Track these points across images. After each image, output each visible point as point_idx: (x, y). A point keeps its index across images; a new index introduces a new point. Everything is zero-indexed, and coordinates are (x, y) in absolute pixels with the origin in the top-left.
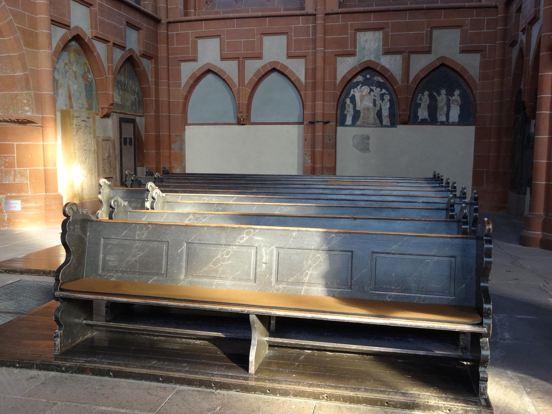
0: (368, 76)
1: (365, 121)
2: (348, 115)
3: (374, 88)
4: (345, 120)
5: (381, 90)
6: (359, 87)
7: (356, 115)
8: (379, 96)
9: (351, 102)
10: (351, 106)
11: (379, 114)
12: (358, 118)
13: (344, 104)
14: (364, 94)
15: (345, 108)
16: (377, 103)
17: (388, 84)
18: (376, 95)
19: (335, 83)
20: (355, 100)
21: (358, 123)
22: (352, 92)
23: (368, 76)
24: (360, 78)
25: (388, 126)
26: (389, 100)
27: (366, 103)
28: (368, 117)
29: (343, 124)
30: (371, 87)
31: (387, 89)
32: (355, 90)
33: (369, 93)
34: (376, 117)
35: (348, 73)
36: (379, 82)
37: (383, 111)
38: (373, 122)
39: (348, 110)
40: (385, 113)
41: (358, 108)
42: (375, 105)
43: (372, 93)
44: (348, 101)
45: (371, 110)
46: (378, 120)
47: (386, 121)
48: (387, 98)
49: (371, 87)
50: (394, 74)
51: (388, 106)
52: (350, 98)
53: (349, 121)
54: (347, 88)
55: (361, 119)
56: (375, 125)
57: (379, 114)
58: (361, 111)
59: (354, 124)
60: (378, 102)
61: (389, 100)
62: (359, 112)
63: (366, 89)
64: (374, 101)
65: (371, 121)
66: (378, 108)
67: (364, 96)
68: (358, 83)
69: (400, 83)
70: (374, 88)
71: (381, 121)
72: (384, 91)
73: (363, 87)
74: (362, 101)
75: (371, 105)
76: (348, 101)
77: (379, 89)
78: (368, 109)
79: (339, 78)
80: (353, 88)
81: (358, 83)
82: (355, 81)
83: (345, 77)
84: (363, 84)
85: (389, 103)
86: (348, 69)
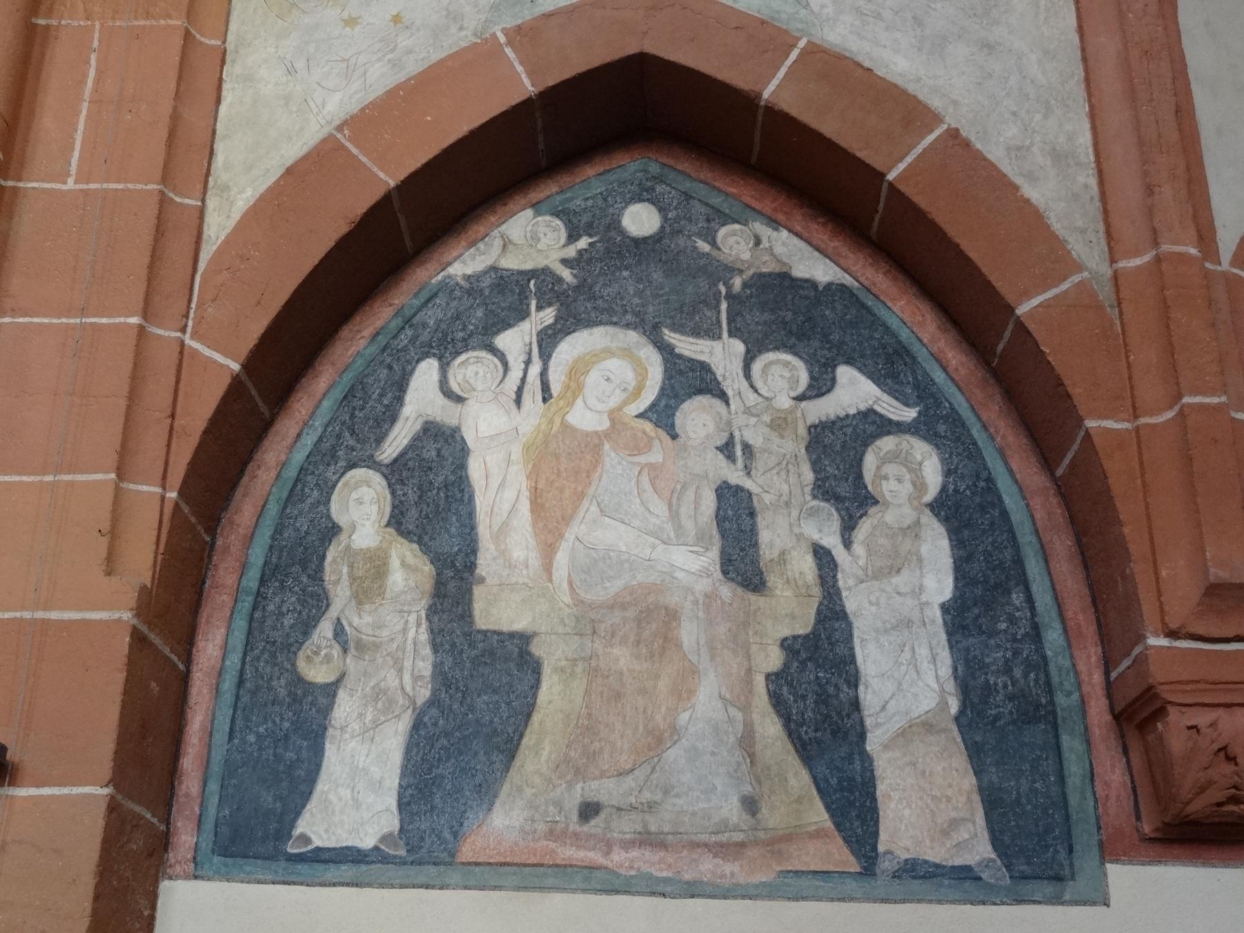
0: (640, 220)
1: (605, 790)
2: (345, 708)
3: (722, 355)
4: (298, 780)
5: (820, 385)
6: (514, 341)
7: (477, 704)
8: (793, 446)
9: (397, 521)
10: (407, 571)
11: (817, 694)
12: (509, 749)
13: (301, 556)
14: (586, 417)
15: (317, 601)
16: (774, 535)
17: (908, 316)
18: (755, 437)
19: (173, 228)
20: (457, 493)
21: (504, 823)
22: (423, 395)
23: (640, 220)
24: (528, 237)
25: (956, 882)
26: (936, 507)
27: (613, 536)
28: (658, 740)
29: (260, 838)
30: (687, 346)
31: (891, 365)
32: (472, 369)
33: (662, 414)
34: (770, 728)
35: (362, 123)
36: (778, 288)
37: (872, 658)
38: (731, 809)
39: (360, 622)
40: (906, 679)
41: (497, 609)
42: (742, 564)
43: (697, 417)
44: (361, 505)
45: (689, 634)
46: (799, 779)
47: (928, 796)
48: (908, 473)
49: (687, 346)
50: (995, 153)
51: (939, 584)
52: (396, 472)
53: (357, 789)
54: (356, 344)
55: (539, 753)
56: (751, 859)
57: (817, 694)
58: (552, 653)
59: (425, 845)
60: (792, 529)
61: (936, 507)
62: (515, 659)
63: (611, 369)
64: (736, 517)
65: (704, 791)
66: (789, 610)
67: (592, 445)
68: (505, 296)
69: (1088, 251)
70: (722, 355)
71: (853, 804)
72: (855, 390)
73: (569, 349)
74: (550, 518)
75: (692, 564)
76: (361, 505)
77: (782, 373)
78: (651, 619)
79: (246, 165)
80: (446, 347)
81: (505, 296)
82: (466, 262)
83: (322, 161)
84: (576, 305)
85: (936, 547)
86: (379, 78)
